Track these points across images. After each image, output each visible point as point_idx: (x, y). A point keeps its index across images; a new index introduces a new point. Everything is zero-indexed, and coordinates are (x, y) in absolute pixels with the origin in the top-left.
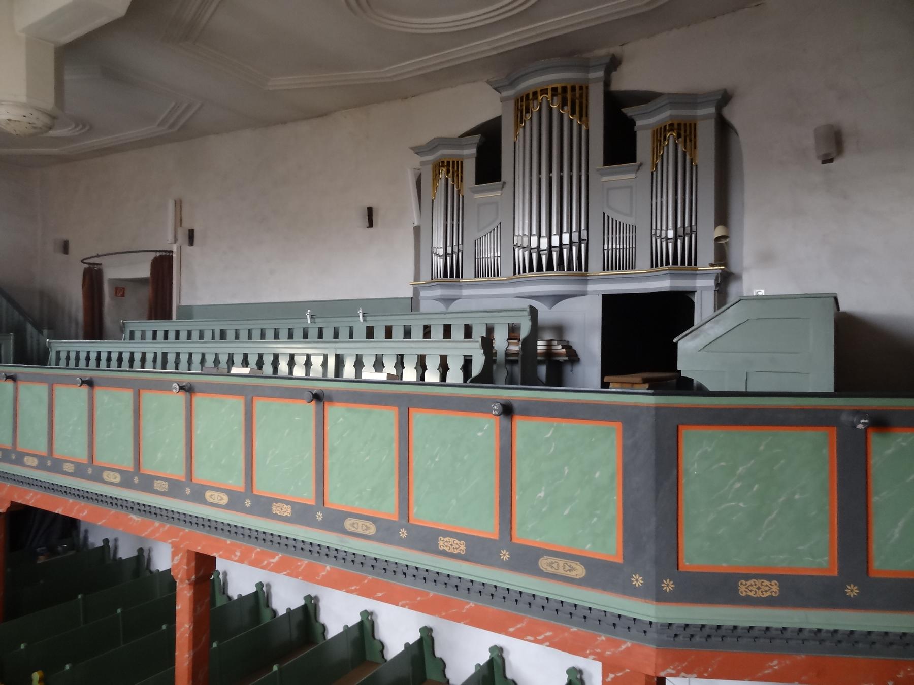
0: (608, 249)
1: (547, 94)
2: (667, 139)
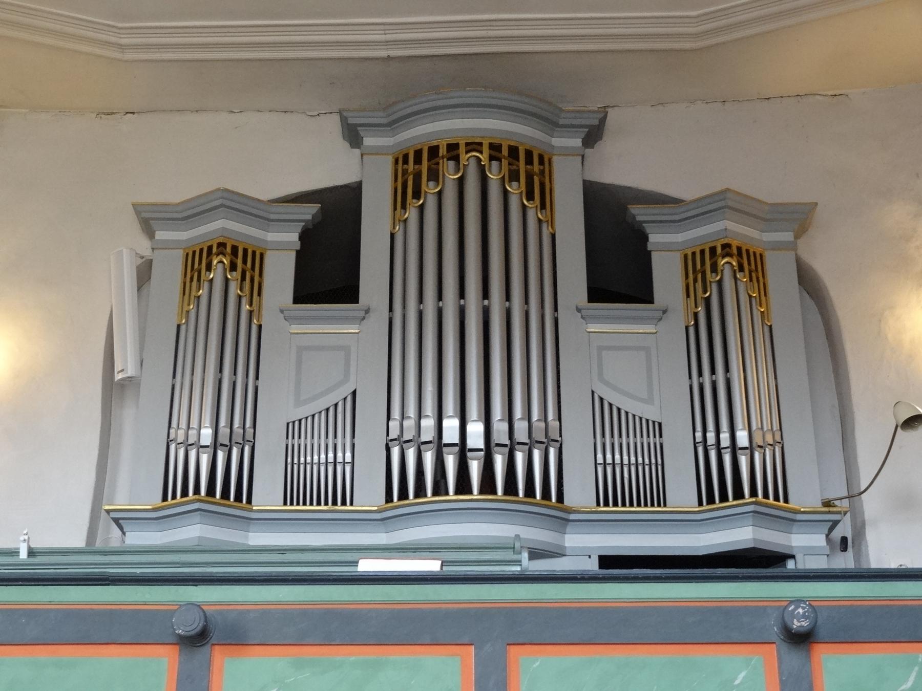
0: (605, 464)
1: (481, 152)
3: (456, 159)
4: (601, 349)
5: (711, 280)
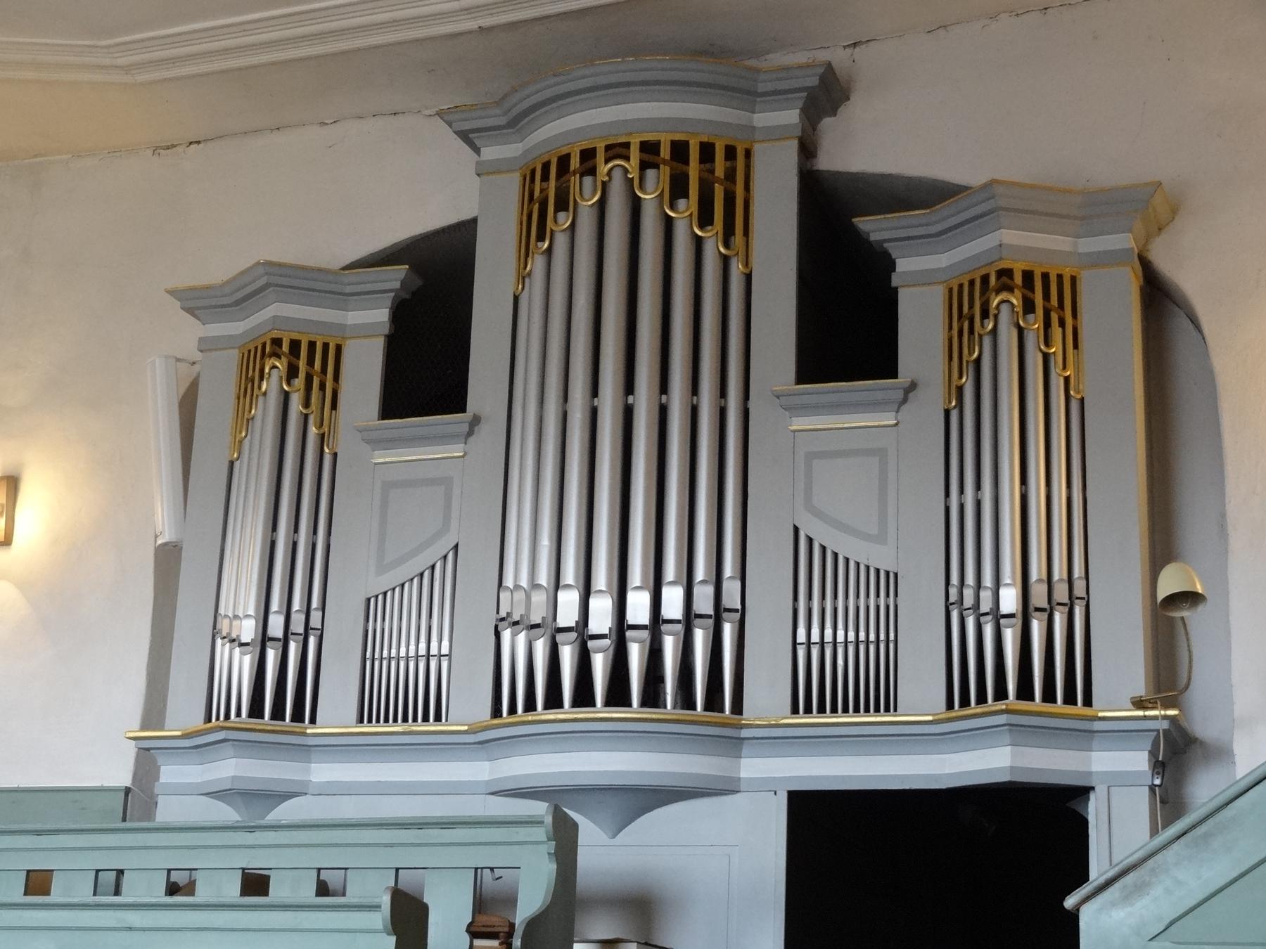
0: (809, 644)
1: (627, 159)
2: (992, 311)
3: (592, 171)
4: (811, 456)
5: (982, 332)
